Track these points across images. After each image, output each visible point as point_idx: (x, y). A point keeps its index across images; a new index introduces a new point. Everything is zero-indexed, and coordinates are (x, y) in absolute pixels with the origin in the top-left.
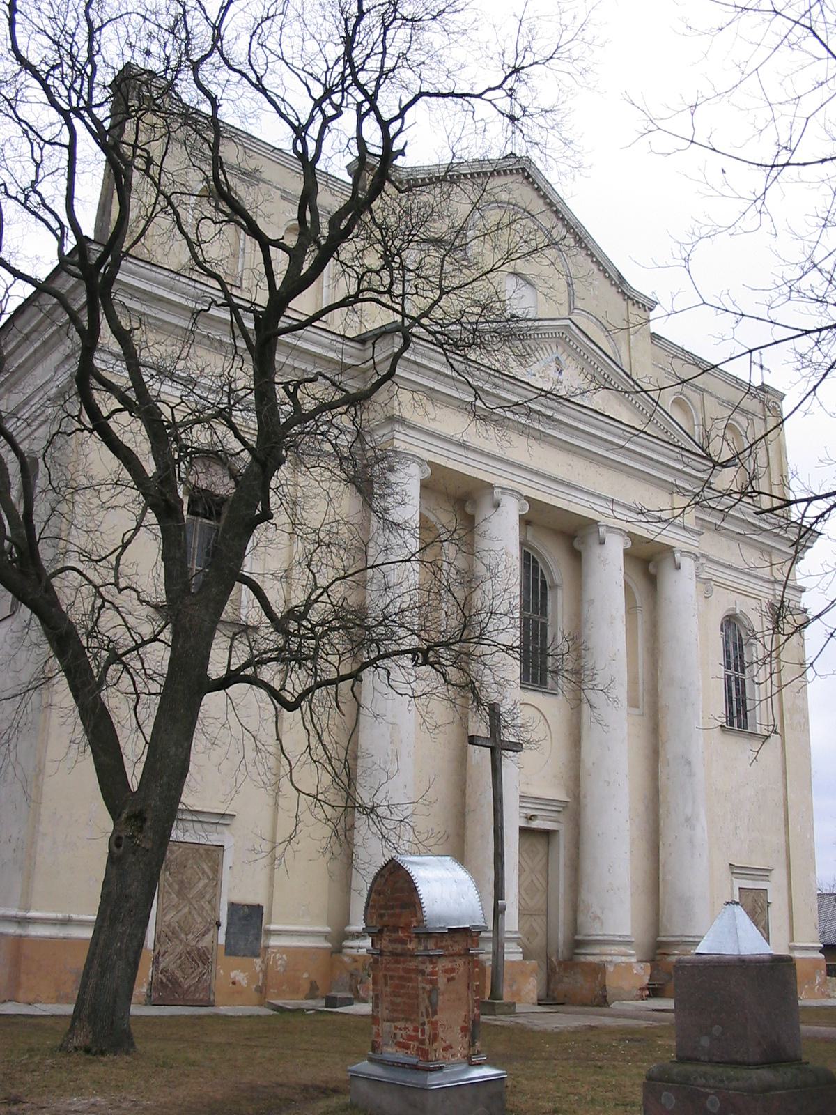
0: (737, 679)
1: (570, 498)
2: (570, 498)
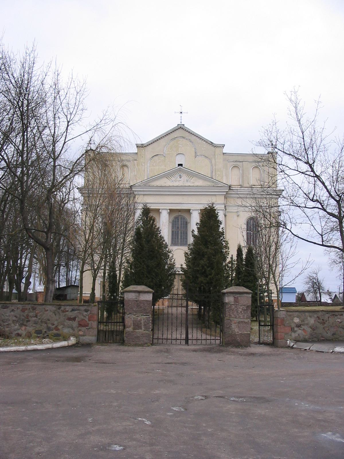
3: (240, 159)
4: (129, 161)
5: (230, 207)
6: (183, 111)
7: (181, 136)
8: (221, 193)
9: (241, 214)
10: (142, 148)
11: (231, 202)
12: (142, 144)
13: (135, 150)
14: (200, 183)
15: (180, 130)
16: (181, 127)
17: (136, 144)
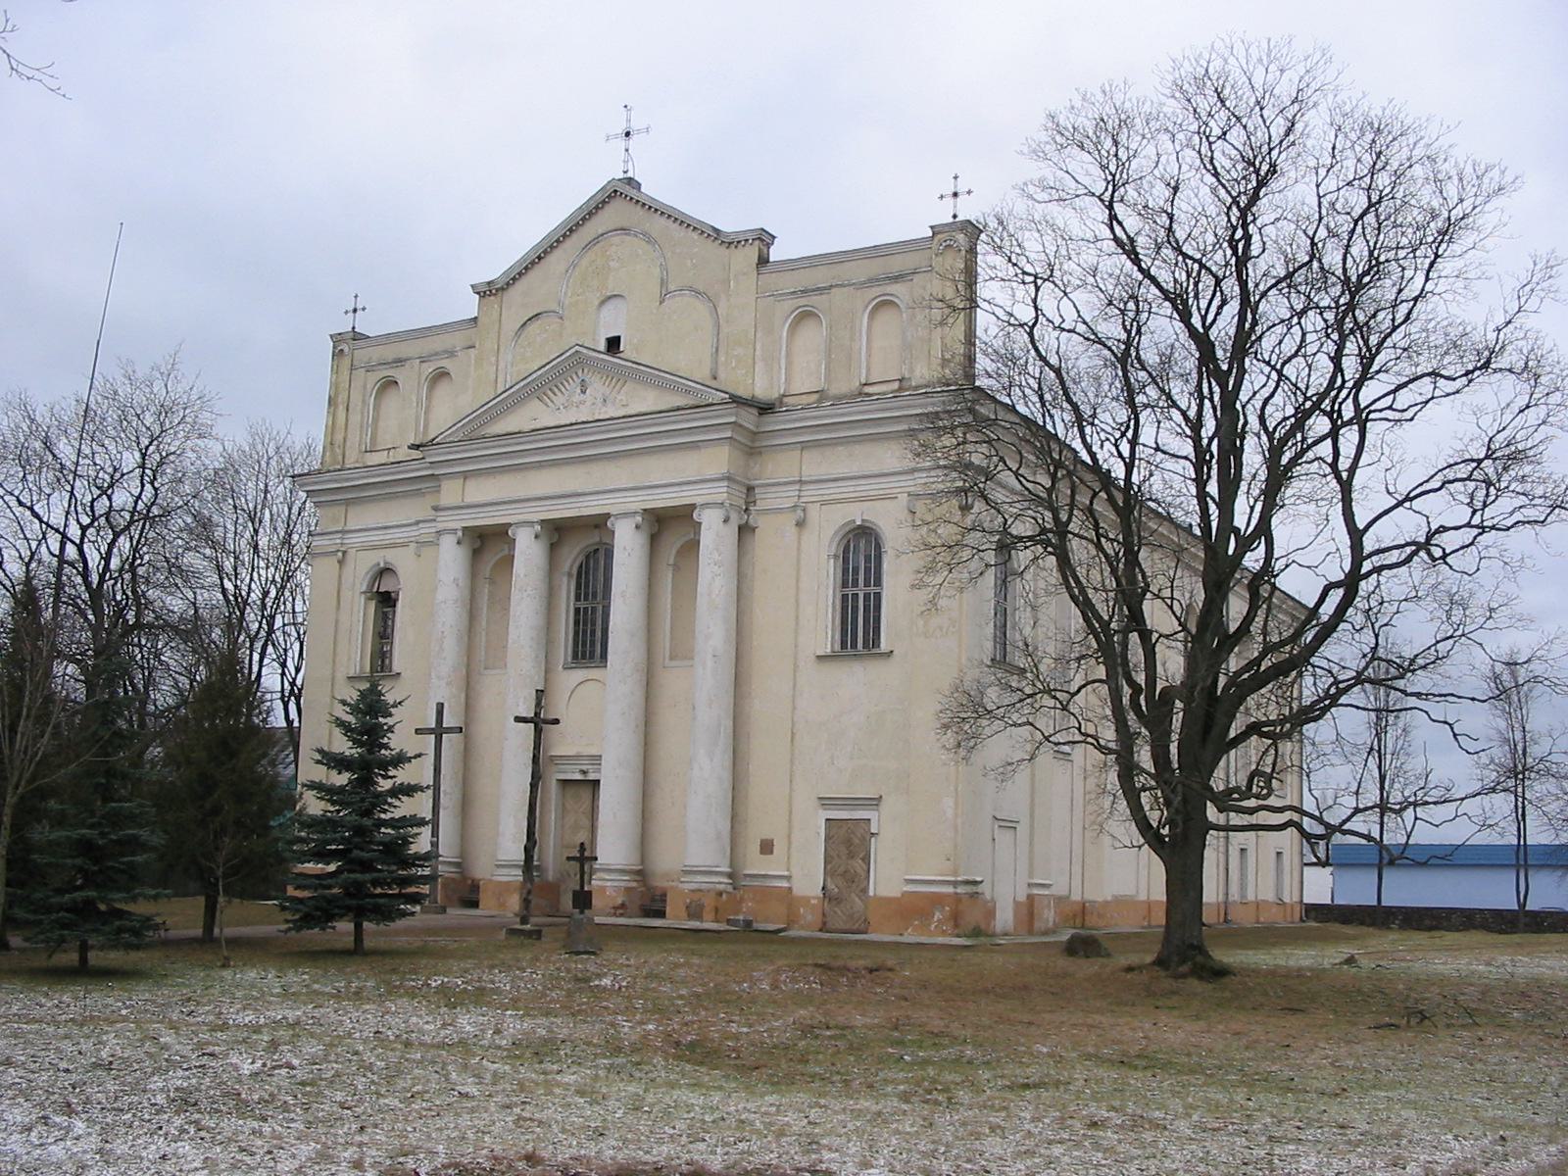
0: (867, 597)
1: (579, 505)
2: (579, 505)
3: (820, 277)
4: (451, 354)
5: (774, 489)
6: (635, 126)
7: (619, 225)
8: (718, 431)
9: (814, 512)
10: (492, 298)
11: (779, 467)
12: (489, 283)
13: (470, 307)
14: (647, 400)
15: (617, 205)
16: (621, 192)
17: (472, 286)
